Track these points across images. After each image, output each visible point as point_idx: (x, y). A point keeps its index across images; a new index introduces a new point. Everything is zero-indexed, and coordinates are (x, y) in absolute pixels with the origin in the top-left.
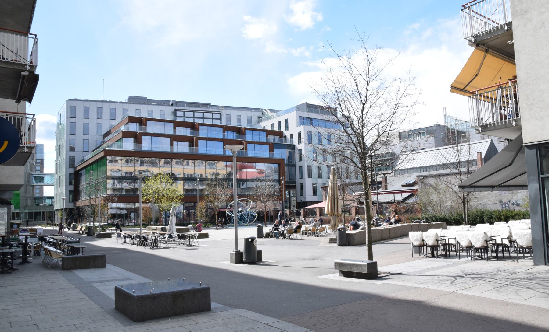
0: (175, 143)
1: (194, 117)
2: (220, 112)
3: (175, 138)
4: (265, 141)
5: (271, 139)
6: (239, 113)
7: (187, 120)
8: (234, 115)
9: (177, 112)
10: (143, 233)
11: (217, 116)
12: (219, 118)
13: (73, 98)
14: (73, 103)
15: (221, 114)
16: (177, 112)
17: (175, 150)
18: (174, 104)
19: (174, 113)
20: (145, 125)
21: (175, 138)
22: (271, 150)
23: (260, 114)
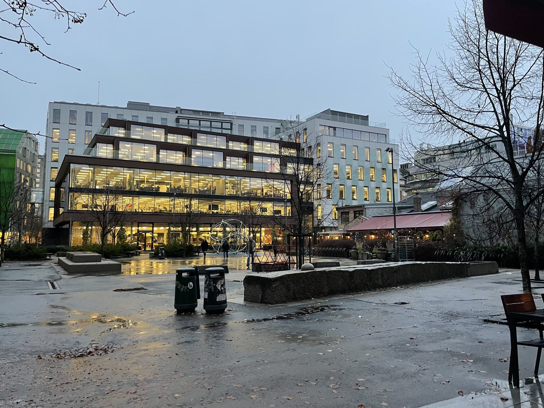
0: (228, 159)
1: (222, 128)
2: (231, 121)
3: (228, 153)
4: (277, 153)
5: (286, 152)
6: (266, 124)
7: (225, 132)
8: (247, 125)
9: (180, 119)
10: (520, 284)
11: (228, 126)
12: (229, 128)
13: (72, 102)
14: (57, 107)
15: (232, 124)
16: (180, 119)
17: (228, 166)
18: (179, 112)
19: (177, 120)
20: (195, 137)
21: (161, 146)
22: (283, 164)
23: (278, 125)
